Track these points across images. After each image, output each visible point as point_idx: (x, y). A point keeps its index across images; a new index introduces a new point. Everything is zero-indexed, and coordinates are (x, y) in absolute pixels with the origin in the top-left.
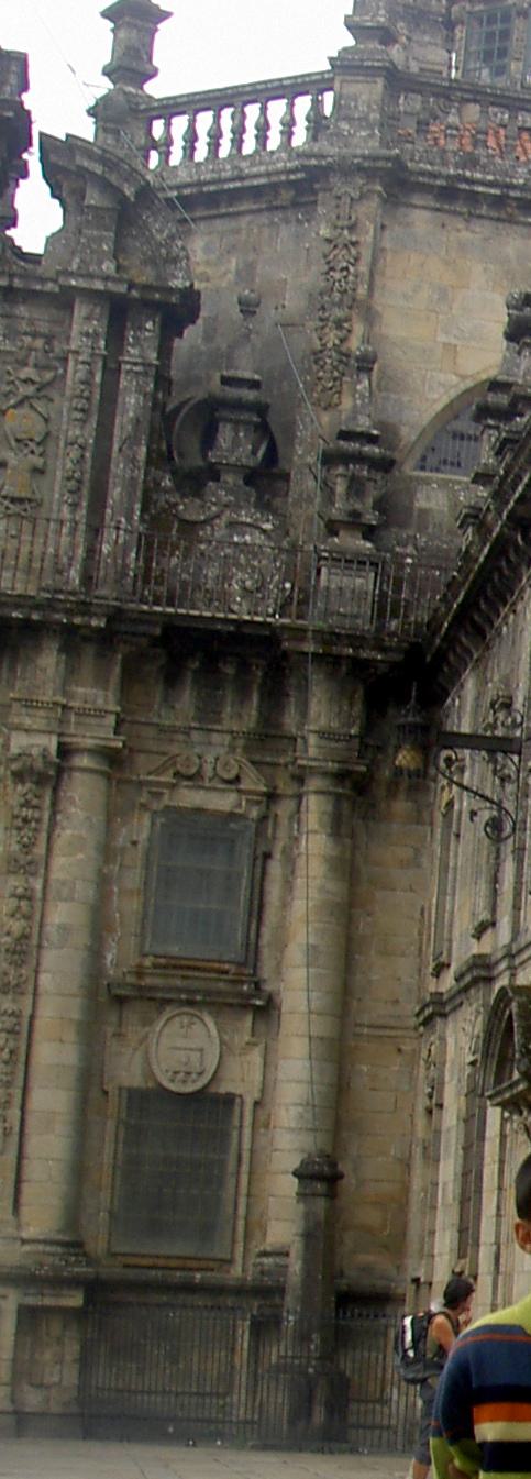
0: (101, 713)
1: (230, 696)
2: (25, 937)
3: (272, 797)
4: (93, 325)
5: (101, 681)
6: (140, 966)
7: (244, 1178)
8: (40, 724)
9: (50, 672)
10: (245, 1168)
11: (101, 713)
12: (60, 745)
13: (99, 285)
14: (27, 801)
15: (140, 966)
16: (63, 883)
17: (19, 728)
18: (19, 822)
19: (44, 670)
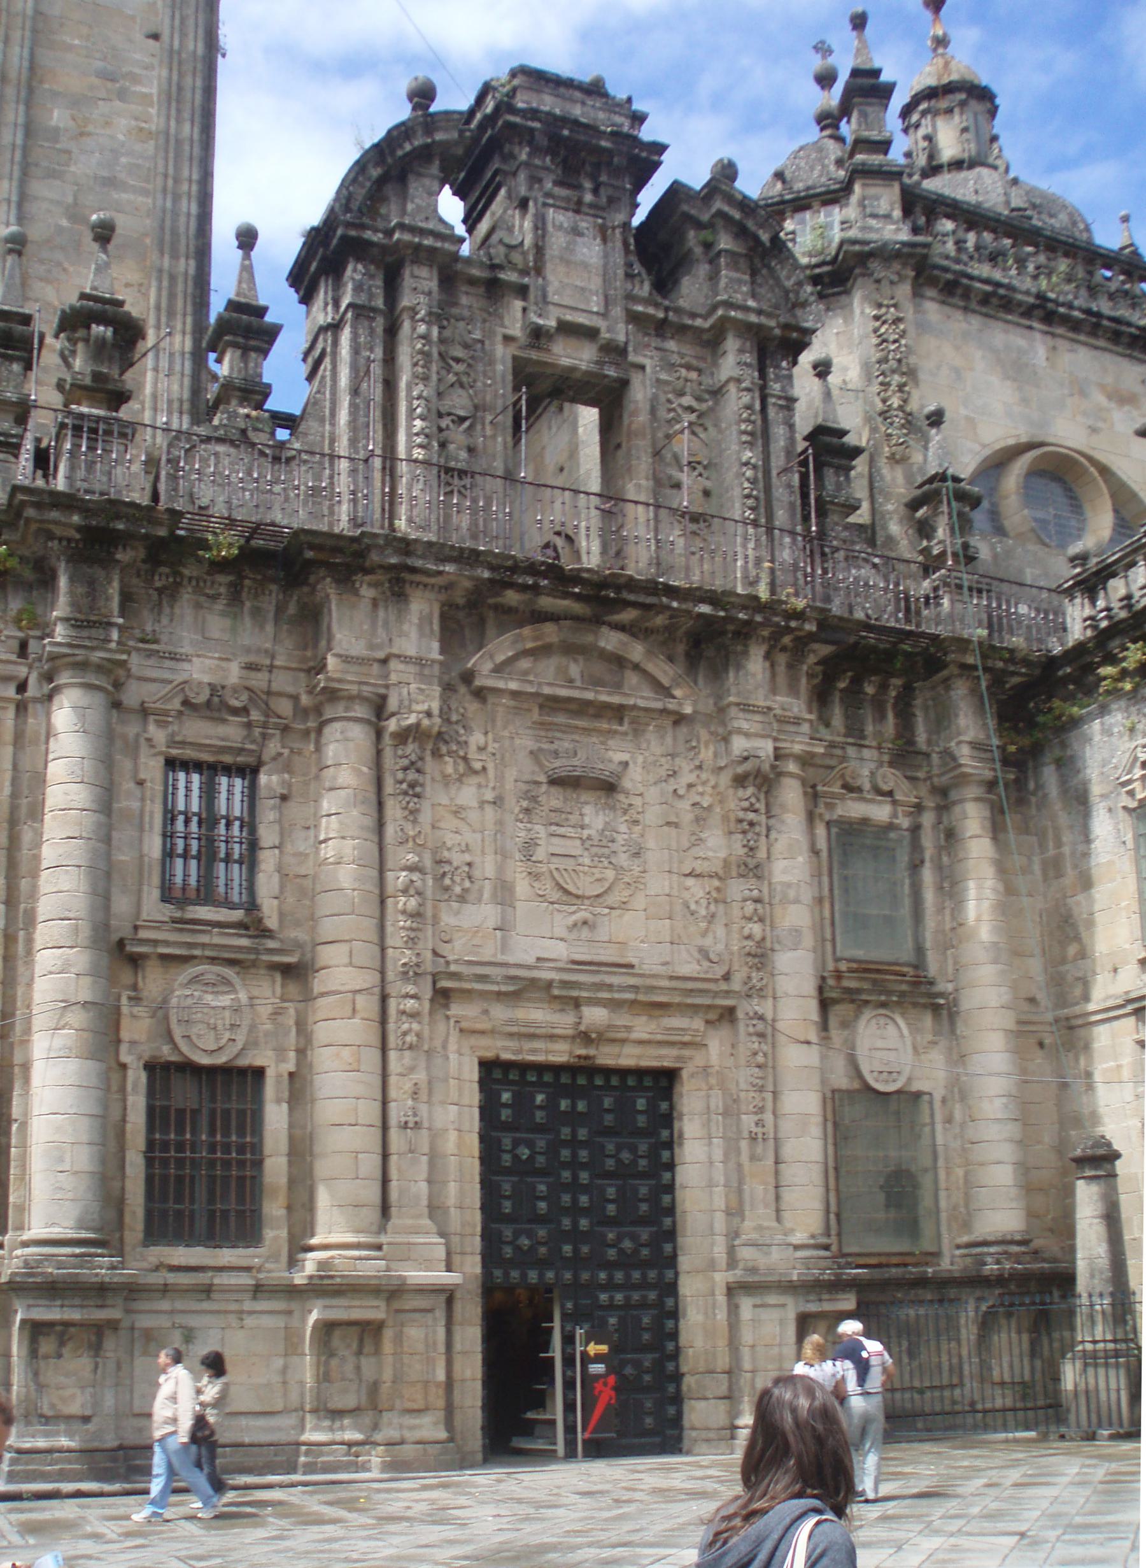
0: (797, 721)
1: (868, 714)
2: (763, 939)
3: (919, 808)
4: (748, 358)
5: (793, 690)
6: (837, 971)
7: (942, 1175)
8: (754, 728)
9: (760, 677)
10: (941, 1163)
11: (797, 721)
12: (776, 749)
13: (753, 318)
14: (752, 804)
15: (837, 971)
16: (789, 885)
17: (739, 731)
18: (745, 826)
19: (754, 675)
